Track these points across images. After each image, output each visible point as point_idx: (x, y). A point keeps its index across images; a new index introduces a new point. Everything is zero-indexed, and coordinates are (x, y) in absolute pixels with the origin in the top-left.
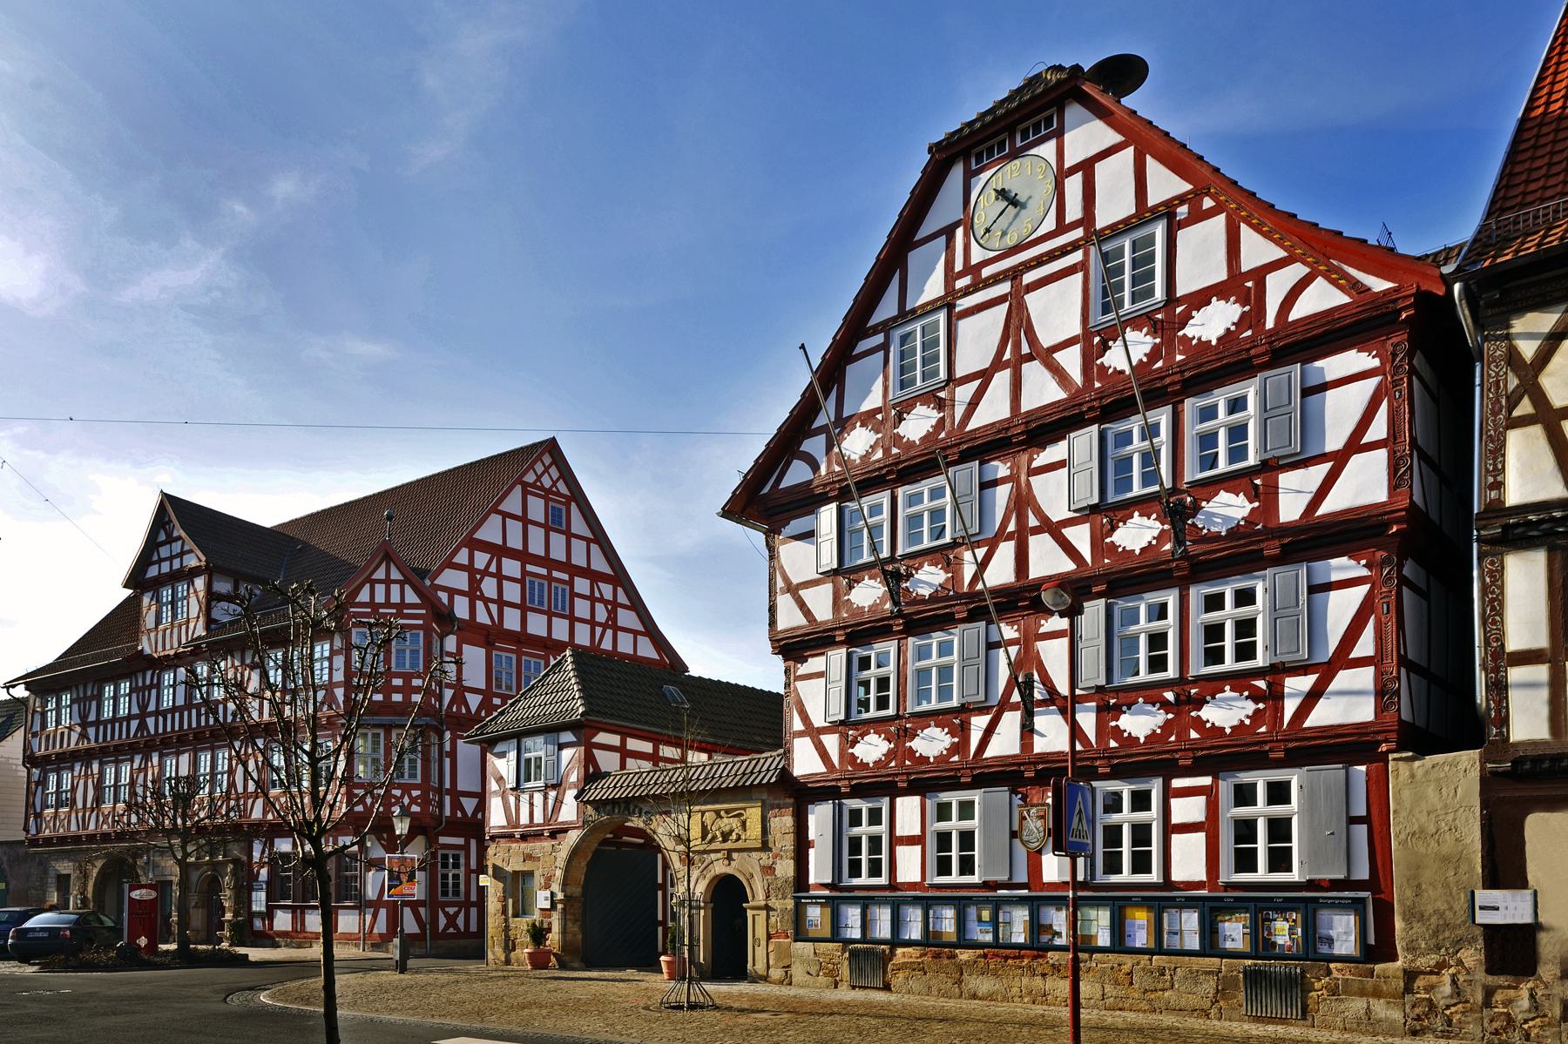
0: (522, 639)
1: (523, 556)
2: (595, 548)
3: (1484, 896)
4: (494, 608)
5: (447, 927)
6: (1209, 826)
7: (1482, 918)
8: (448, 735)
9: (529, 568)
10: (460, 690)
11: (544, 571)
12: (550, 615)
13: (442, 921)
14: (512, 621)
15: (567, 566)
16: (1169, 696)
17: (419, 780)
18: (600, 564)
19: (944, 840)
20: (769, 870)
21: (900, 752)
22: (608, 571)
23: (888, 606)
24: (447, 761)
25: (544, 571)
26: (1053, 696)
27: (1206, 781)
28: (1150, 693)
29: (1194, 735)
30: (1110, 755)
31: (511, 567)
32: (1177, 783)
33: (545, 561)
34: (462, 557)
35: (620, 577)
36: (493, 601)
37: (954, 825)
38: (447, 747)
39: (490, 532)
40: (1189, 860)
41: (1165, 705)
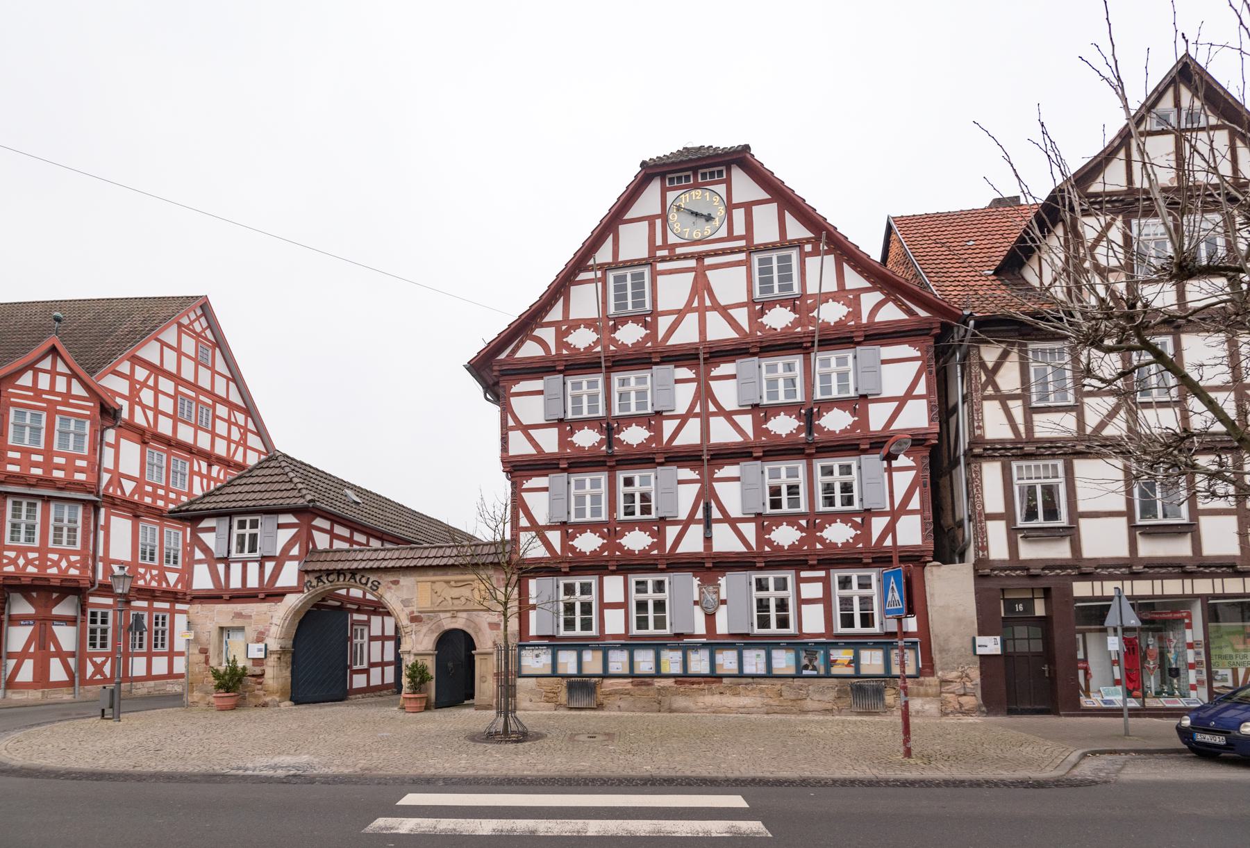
0: (170, 443)
1: (176, 378)
2: (232, 385)
3: (980, 640)
4: (150, 414)
5: (94, 674)
7: (980, 651)
8: (103, 511)
9: (181, 389)
10: (117, 477)
11: (193, 394)
12: (197, 428)
13: (90, 669)
14: (165, 427)
15: (211, 394)
16: (803, 522)
17: (78, 547)
18: (235, 398)
22: (241, 404)
23: (604, 448)
24: (101, 534)
25: (193, 394)
26: (727, 519)
27: (822, 574)
28: (792, 519)
29: (819, 546)
30: (761, 554)
31: (166, 385)
32: (804, 574)
33: (194, 386)
34: (125, 367)
35: (249, 410)
36: (150, 408)
38: (102, 521)
39: (150, 352)
41: (801, 528)
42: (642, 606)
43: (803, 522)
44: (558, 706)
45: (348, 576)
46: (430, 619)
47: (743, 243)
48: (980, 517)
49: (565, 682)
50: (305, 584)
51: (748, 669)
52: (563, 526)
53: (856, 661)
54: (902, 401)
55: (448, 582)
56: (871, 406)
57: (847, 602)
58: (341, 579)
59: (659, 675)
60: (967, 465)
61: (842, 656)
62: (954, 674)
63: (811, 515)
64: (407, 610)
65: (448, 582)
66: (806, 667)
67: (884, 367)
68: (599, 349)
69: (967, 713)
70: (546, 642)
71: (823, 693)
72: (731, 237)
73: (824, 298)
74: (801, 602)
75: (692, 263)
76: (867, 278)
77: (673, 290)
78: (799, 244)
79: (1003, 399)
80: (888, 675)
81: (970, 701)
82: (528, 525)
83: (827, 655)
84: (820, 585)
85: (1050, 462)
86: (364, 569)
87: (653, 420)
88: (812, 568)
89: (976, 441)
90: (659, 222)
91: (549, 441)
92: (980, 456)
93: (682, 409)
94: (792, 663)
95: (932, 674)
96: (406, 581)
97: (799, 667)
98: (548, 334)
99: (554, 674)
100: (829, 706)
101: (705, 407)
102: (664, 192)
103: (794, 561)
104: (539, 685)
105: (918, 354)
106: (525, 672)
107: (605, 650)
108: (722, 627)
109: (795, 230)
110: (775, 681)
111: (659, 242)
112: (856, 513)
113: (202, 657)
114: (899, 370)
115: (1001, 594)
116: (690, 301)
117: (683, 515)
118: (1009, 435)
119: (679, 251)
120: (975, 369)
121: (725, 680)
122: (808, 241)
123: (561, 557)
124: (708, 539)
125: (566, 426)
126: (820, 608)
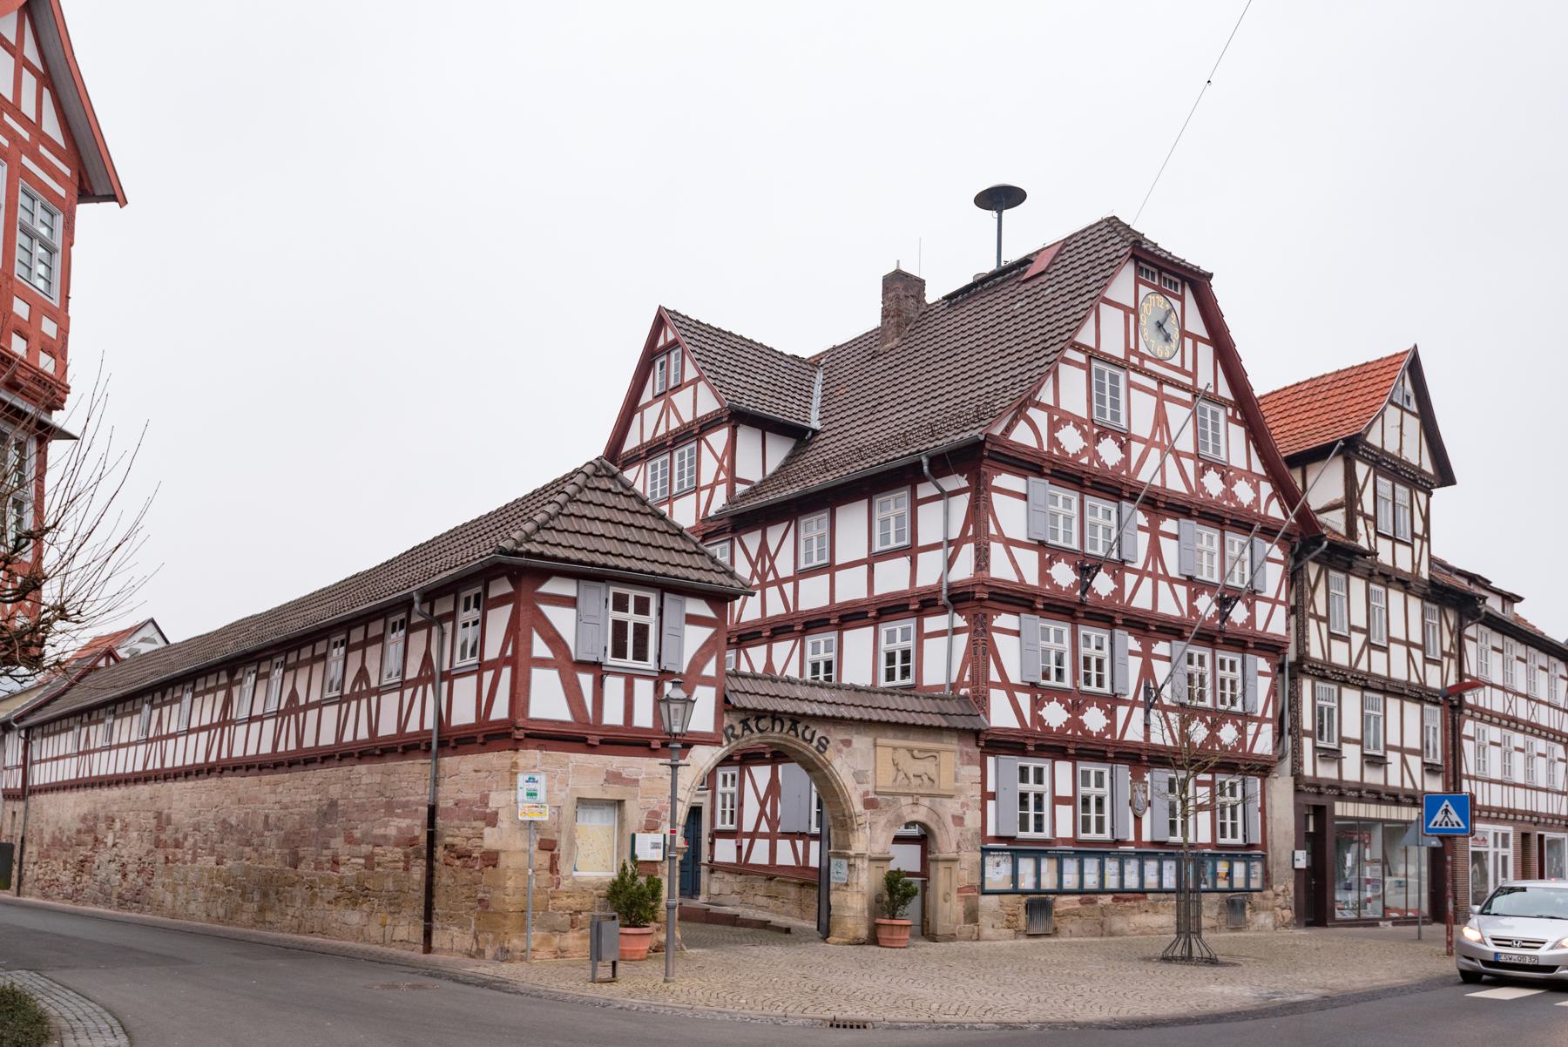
20: (959, 820)
27: (1208, 777)
37: (1092, 791)
42: (1086, 801)
45: (788, 725)
48: (1297, 732)
52: (1032, 687)
55: (910, 750)
58: (777, 729)
63: (1213, 712)
64: (862, 788)
65: (910, 750)
70: (1004, 845)
79: (1319, 619)
82: (998, 680)
101: (1155, 567)
113: (545, 858)
116: (1153, 434)
117: (1130, 697)
125: (1048, 552)
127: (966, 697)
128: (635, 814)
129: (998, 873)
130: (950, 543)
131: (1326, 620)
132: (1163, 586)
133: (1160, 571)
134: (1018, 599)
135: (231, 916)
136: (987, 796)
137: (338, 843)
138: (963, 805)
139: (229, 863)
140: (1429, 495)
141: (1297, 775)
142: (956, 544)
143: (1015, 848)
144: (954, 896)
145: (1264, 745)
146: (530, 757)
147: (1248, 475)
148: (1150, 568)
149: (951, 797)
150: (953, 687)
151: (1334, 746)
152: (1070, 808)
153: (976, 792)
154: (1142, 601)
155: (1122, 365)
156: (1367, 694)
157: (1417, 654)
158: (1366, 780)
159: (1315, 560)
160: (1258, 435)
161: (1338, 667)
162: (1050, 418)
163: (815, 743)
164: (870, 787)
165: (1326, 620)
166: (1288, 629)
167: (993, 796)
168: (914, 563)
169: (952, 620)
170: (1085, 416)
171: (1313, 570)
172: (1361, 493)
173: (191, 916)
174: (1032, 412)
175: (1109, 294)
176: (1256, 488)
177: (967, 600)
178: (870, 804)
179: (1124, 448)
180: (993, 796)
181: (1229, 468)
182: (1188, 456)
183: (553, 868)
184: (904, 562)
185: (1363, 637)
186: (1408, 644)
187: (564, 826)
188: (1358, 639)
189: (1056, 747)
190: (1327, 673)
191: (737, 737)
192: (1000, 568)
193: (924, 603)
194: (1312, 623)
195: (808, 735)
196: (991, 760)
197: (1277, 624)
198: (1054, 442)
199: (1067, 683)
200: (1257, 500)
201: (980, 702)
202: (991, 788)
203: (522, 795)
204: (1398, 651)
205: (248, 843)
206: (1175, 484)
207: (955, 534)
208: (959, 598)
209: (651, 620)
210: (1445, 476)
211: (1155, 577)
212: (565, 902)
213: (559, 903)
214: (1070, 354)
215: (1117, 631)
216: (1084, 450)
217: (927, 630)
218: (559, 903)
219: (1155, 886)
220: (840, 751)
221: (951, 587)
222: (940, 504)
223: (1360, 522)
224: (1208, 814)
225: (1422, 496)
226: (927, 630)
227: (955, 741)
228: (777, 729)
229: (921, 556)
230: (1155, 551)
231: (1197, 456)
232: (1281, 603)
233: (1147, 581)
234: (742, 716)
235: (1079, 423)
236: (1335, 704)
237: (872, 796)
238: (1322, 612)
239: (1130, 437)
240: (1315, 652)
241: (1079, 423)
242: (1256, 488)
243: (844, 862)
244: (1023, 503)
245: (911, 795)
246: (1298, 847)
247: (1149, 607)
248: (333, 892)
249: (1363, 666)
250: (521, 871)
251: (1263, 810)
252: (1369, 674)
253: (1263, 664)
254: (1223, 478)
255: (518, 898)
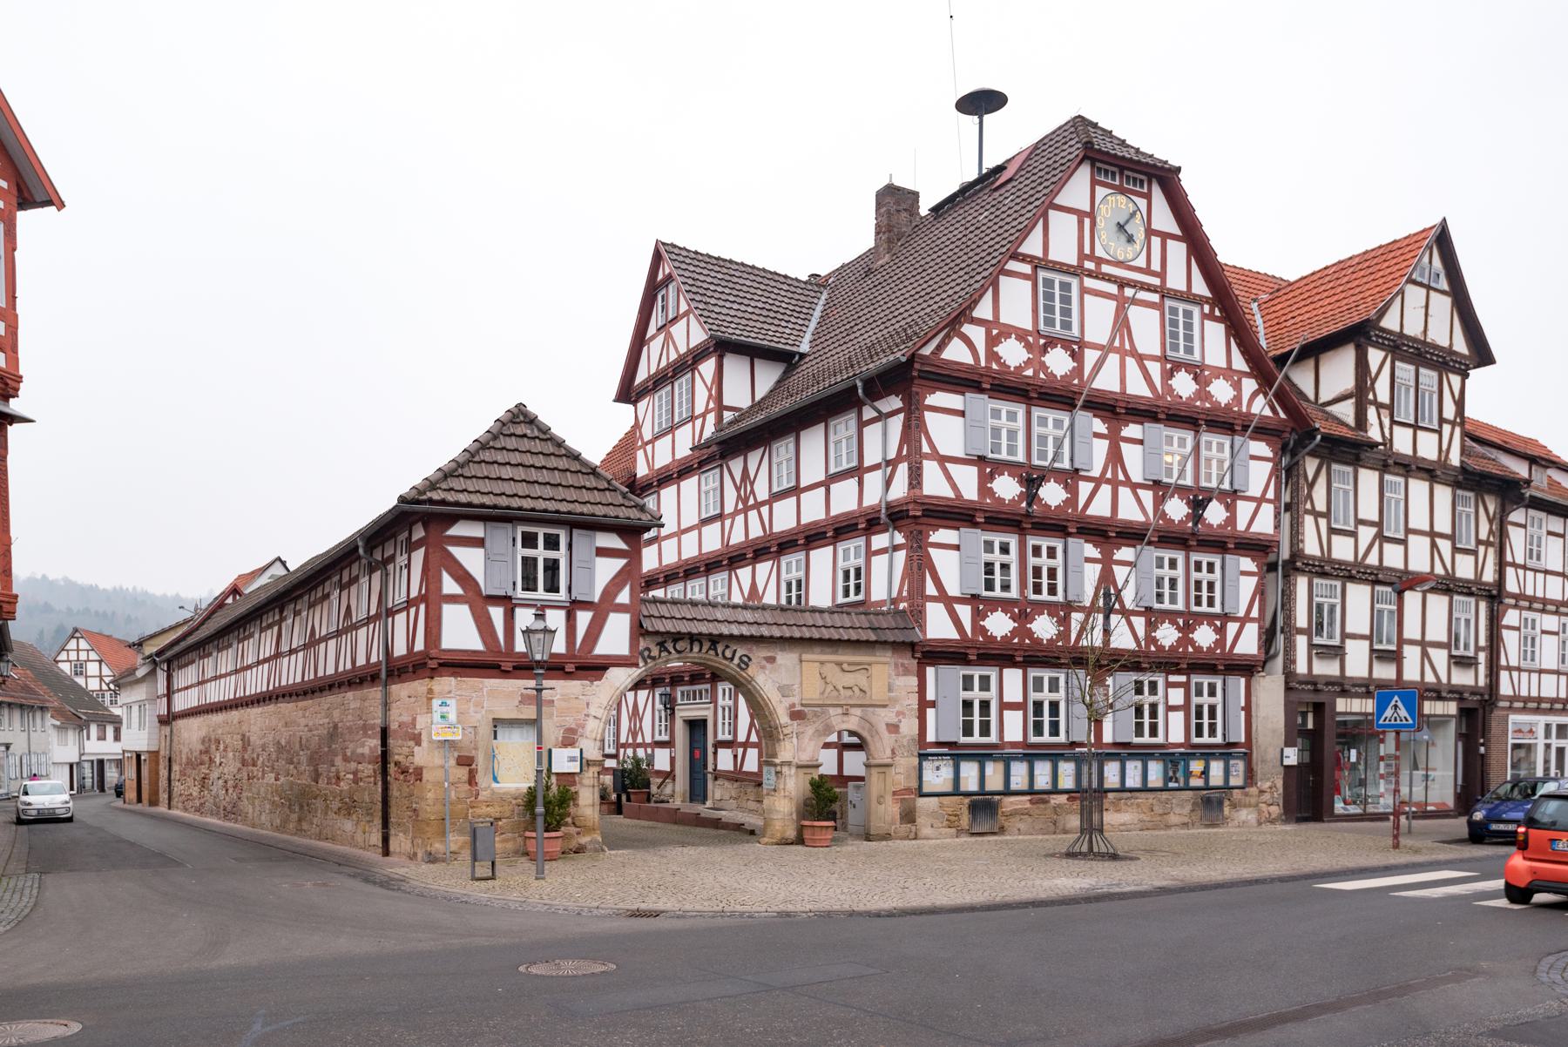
6: (1185, 707)
7: (1287, 762)
16: (1181, 622)
19: (1038, 706)
20: (894, 728)
21: (1022, 631)
27: (1183, 679)
30: (1147, 654)
32: (1172, 678)
37: (1046, 696)
40: (1175, 730)
41: (1179, 629)
43: (1181, 622)
44: (960, 832)
45: (707, 645)
46: (816, 715)
47: (1156, 281)
48: (1290, 630)
49: (967, 801)
50: (641, 654)
51: (1130, 783)
52: (974, 599)
53: (1205, 773)
54: (1260, 501)
55: (839, 664)
56: (1240, 503)
57: (1199, 708)
58: (696, 649)
59: (1055, 791)
60: (1286, 576)
61: (1196, 766)
62: (1269, 784)
63: (1187, 614)
64: (787, 702)
65: (839, 664)
66: (1171, 779)
67: (1252, 462)
68: (1029, 372)
69: (1272, 822)
71: (1182, 807)
72: (1147, 271)
73: (1218, 373)
74: (1170, 708)
75: (1112, 289)
76: (1247, 361)
77: (1097, 319)
78: (1197, 300)
79: (1317, 515)
80: (1227, 787)
81: (1276, 810)
83: (1187, 766)
84: (1182, 690)
85: (1334, 583)
86: (731, 637)
87: (1070, 478)
88: (1179, 672)
89: (1297, 554)
90: (1087, 221)
91: (968, 483)
92: (1297, 569)
93: (1096, 473)
94: (1161, 775)
95: (1251, 785)
96: (786, 659)
97: (1167, 779)
98: (977, 334)
99: (956, 792)
100: (1186, 820)
101: (1115, 473)
102: (1094, 183)
103: (1168, 663)
104: (941, 806)
105: (1271, 455)
106: (926, 789)
107: (1007, 760)
108: (1107, 737)
109: (1200, 287)
110: (1149, 795)
111: (1087, 251)
112: (1216, 616)
113: (463, 773)
114: (1258, 468)
115: (1311, 707)
116: (1112, 340)
118: (1318, 553)
119: (1105, 269)
120: (1302, 481)
121: (1110, 795)
122: (1207, 301)
123: (972, 641)
124: (1107, 632)
125: (988, 467)
126: (1181, 714)
127: (904, 611)
128: (552, 731)
129: (938, 776)
130: (888, 463)
131: (1327, 515)
132: (1124, 492)
133: (1121, 477)
134: (956, 514)
135: (282, 828)
136: (924, 704)
137: (338, 761)
138: (898, 714)
139: (282, 779)
140: (1465, 376)
141: (1289, 674)
142: (892, 464)
143: (956, 753)
144: (889, 798)
145: (1248, 643)
146: (446, 683)
147: (1228, 372)
148: (1109, 475)
149: (885, 706)
150: (894, 602)
151: (1336, 642)
152: (1020, 713)
153: (914, 701)
154: (1100, 508)
155: (1077, 271)
156: (1378, 588)
157: (1445, 546)
158: (1375, 675)
159: (1313, 454)
160: (1239, 331)
161: (1340, 563)
162: (988, 333)
163: (736, 661)
164: (796, 700)
165: (1327, 515)
166: (1277, 526)
167: (933, 704)
168: (861, 483)
169: (892, 537)
170: (1030, 328)
171: (1311, 465)
172: (1374, 381)
173: (262, 826)
174: (967, 329)
175: (1058, 201)
176: (1237, 386)
177: (902, 518)
178: (796, 715)
179: (1077, 356)
180: (933, 704)
181: (1202, 367)
182: (1154, 358)
183: (472, 780)
184: (852, 483)
185: (1374, 530)
186: (1433, 534)
187: (481, 744)
188: (1366, 534)
189: (1000, 655)
190: (1325, 568)
191: (654, 658)
192: (935, 485)
193: (864, 524)
194: (1309, 520)
195: (728, 654)
196: (930, 671)
197: (1264, 524)
198: (992, 356)
199: (1014, 593)
200: (1238, 399)
201: (917, 615)
202: (930, 696)
203: (436, 717)
204: (1420, 545)
205: (291, 763)
206: (1137, 387)
207: (892, 455)
208: (896, 516)
209: (561, 555)
210: (1482, 355)
211: (1115, 484)
212: (484, 810)
213: (478, 811)
214: (1013, 265)
215: (1070, 540)
216: (1028, 363)
217: (874, 547)
218: (478, 811)
219: (1117, 785)
220: (763, 668)
221: (889, 506)
222: (879, 425)
223: (1372, 412)
224: (1181, 714)
225: (1455, 380)
226: (874, 547)
227: (889, 654)
228: (696, 649)
229: (867, 476)
230: (1115, 457)
231: (1163, 359)
232: (1269, 501)
233: (1106, 490)
234: (660, 639)
235: (1021, 335)
236: (1338, 601)
237: (798, 708)
238: (1321, 506)
239: (1082, 344)
240: (1311, 547)
241: (1021, 335)
242: (1237, 386)
243: (773, 769)
244: (960, 419)
245: (841, 706)
246: (1289, 742)
247: (1108, 514)
248: (336, 805)
249: (1373, 560)
250: (439, 784)
251: (1248, 709)
252: (1381, 567)
253: (1247, 564)
254: (1196, 379)
255: (439, 807)
